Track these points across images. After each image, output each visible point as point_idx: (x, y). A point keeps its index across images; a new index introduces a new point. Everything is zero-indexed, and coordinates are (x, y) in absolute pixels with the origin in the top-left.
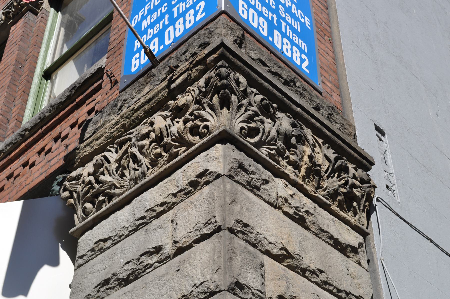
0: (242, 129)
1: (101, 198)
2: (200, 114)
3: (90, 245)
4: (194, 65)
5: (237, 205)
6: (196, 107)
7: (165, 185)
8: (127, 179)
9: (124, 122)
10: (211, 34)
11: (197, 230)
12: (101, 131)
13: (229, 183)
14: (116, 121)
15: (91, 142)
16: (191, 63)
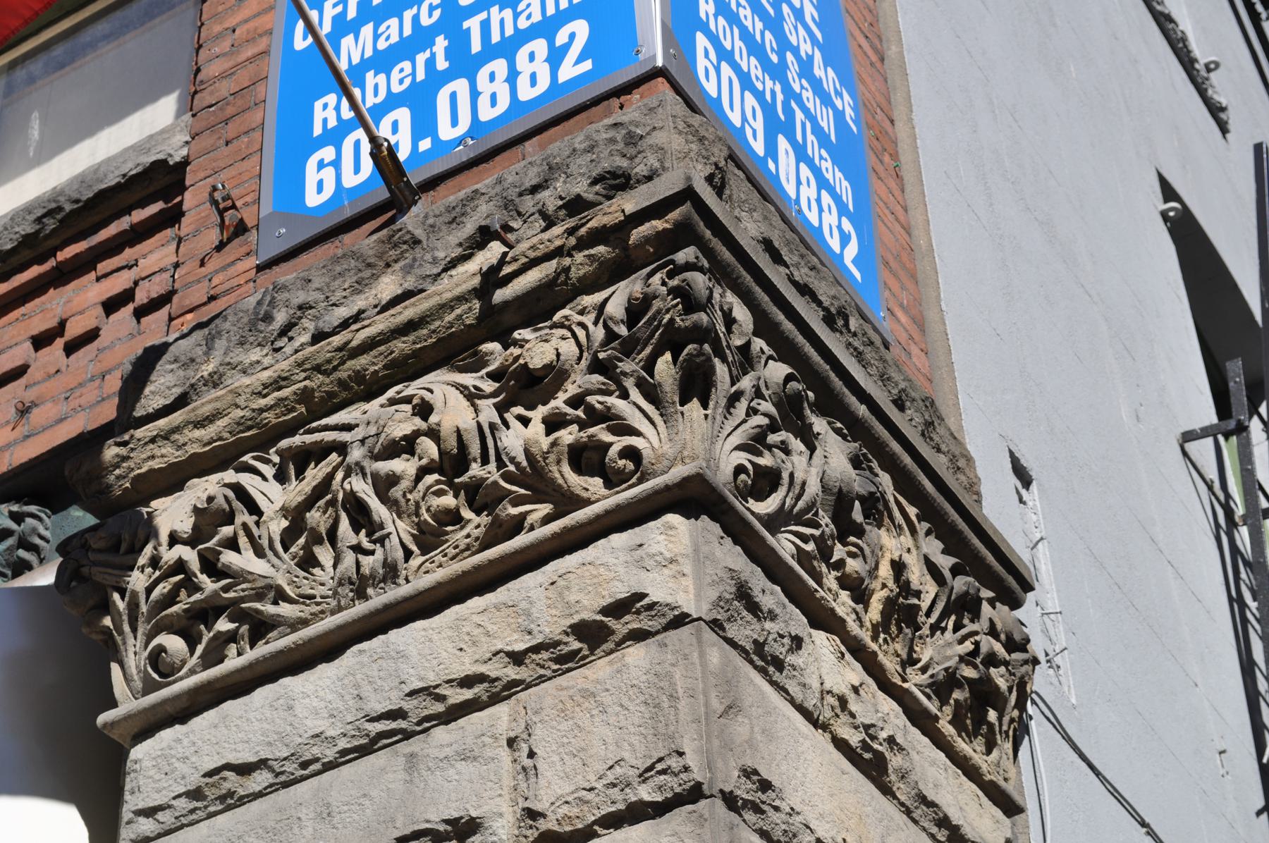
0: (740, 469)
1: (223, 625)
2: (609, 408)
3: (183, 778)
4: (579, 239)
5: (740, 719)
6: (594, 381)
7: (477, 619)
8: (325, 574)
9: (307, 383)
10: (635, 144)
11: (614, 785)
12: (217, 399)
13: (714, 645)
14: (276, 375)
15: (177, 429)
16: (571, 232)
